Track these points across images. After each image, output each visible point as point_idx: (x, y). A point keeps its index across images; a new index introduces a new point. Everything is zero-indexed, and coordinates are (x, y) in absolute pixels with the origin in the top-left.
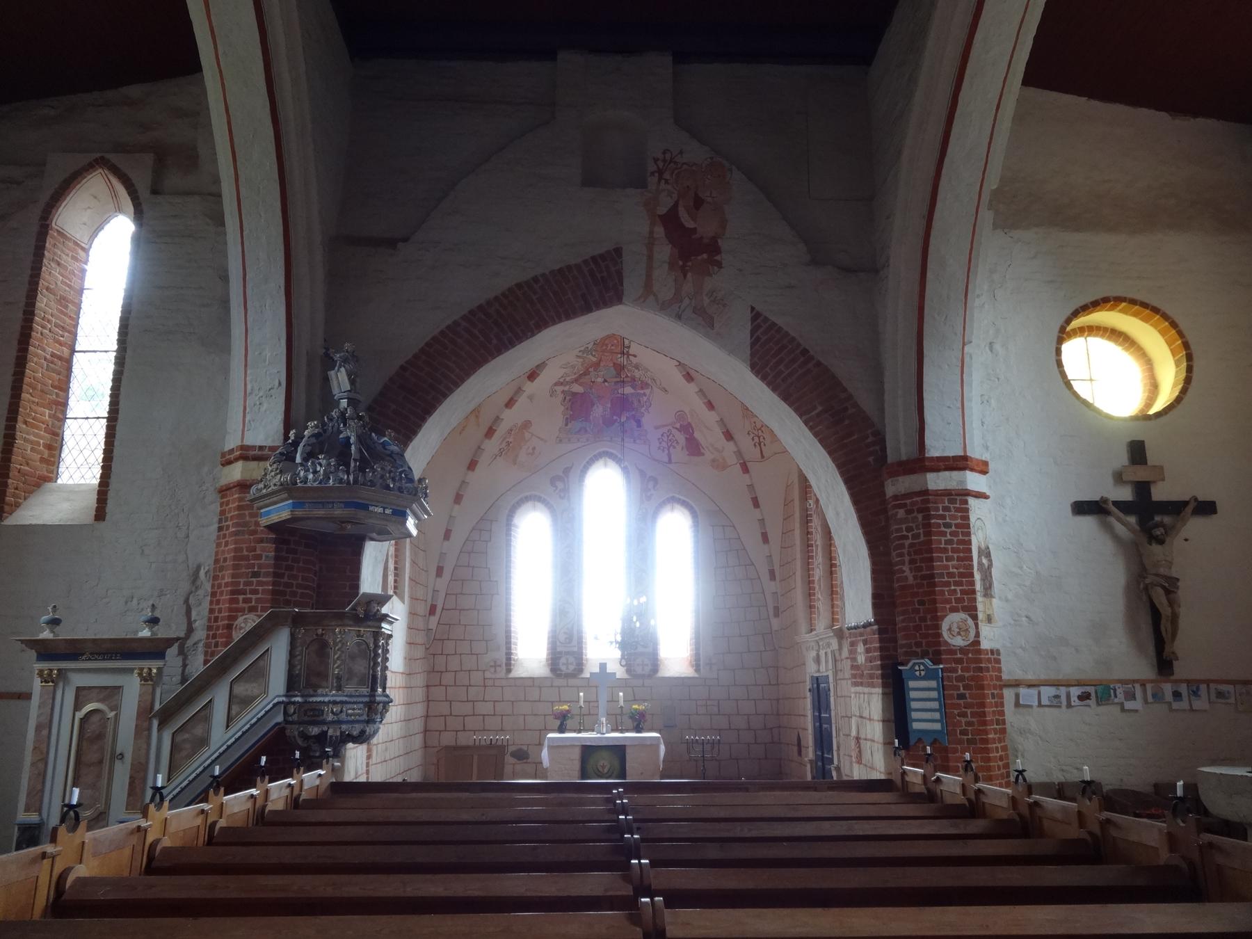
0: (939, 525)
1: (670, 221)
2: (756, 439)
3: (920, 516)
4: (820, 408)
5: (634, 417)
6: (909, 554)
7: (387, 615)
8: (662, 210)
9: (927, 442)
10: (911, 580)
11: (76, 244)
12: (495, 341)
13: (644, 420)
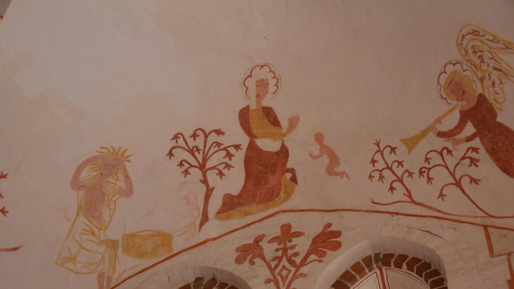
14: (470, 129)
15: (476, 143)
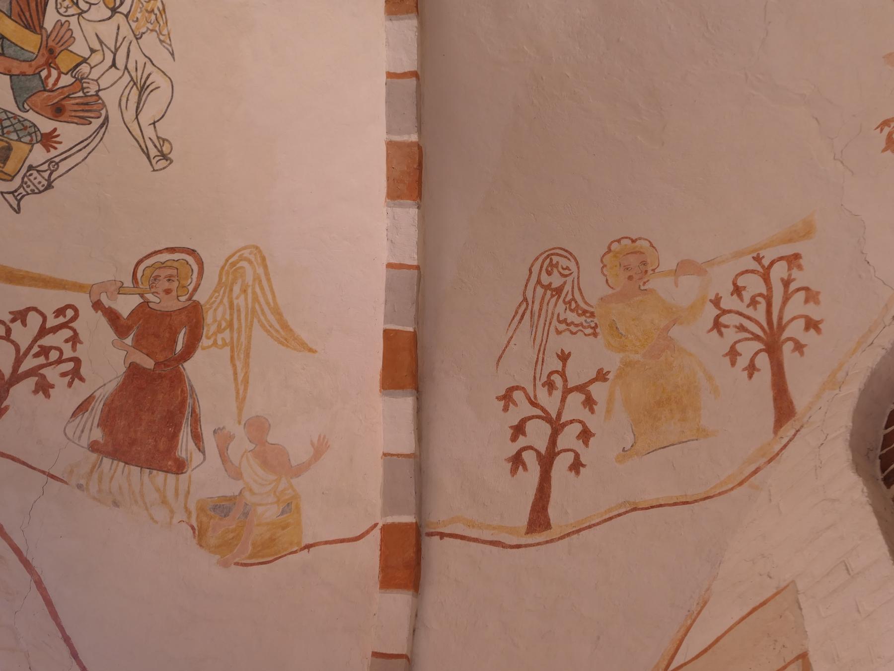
2: (538, 435)
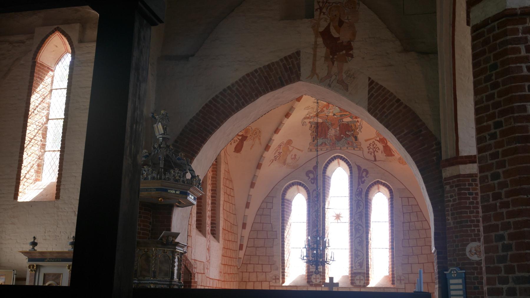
0: (465, 194)
1: (326, 35)
3: (456, 189)
4: (406, 131)
5: (353, 135)
6: (451, 210)
7: (178, 243)
8: (321, 29)
9: (460, 148)
10: (452, 225)
11: (49, 68)
12: (235, 104)
13: (359, 136)
14: (240, 138)
15: (238, 141)
